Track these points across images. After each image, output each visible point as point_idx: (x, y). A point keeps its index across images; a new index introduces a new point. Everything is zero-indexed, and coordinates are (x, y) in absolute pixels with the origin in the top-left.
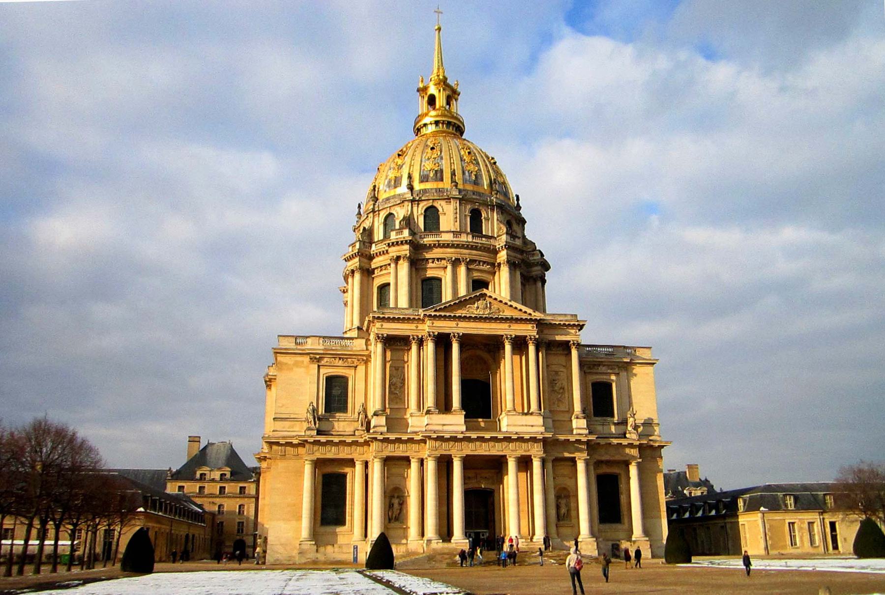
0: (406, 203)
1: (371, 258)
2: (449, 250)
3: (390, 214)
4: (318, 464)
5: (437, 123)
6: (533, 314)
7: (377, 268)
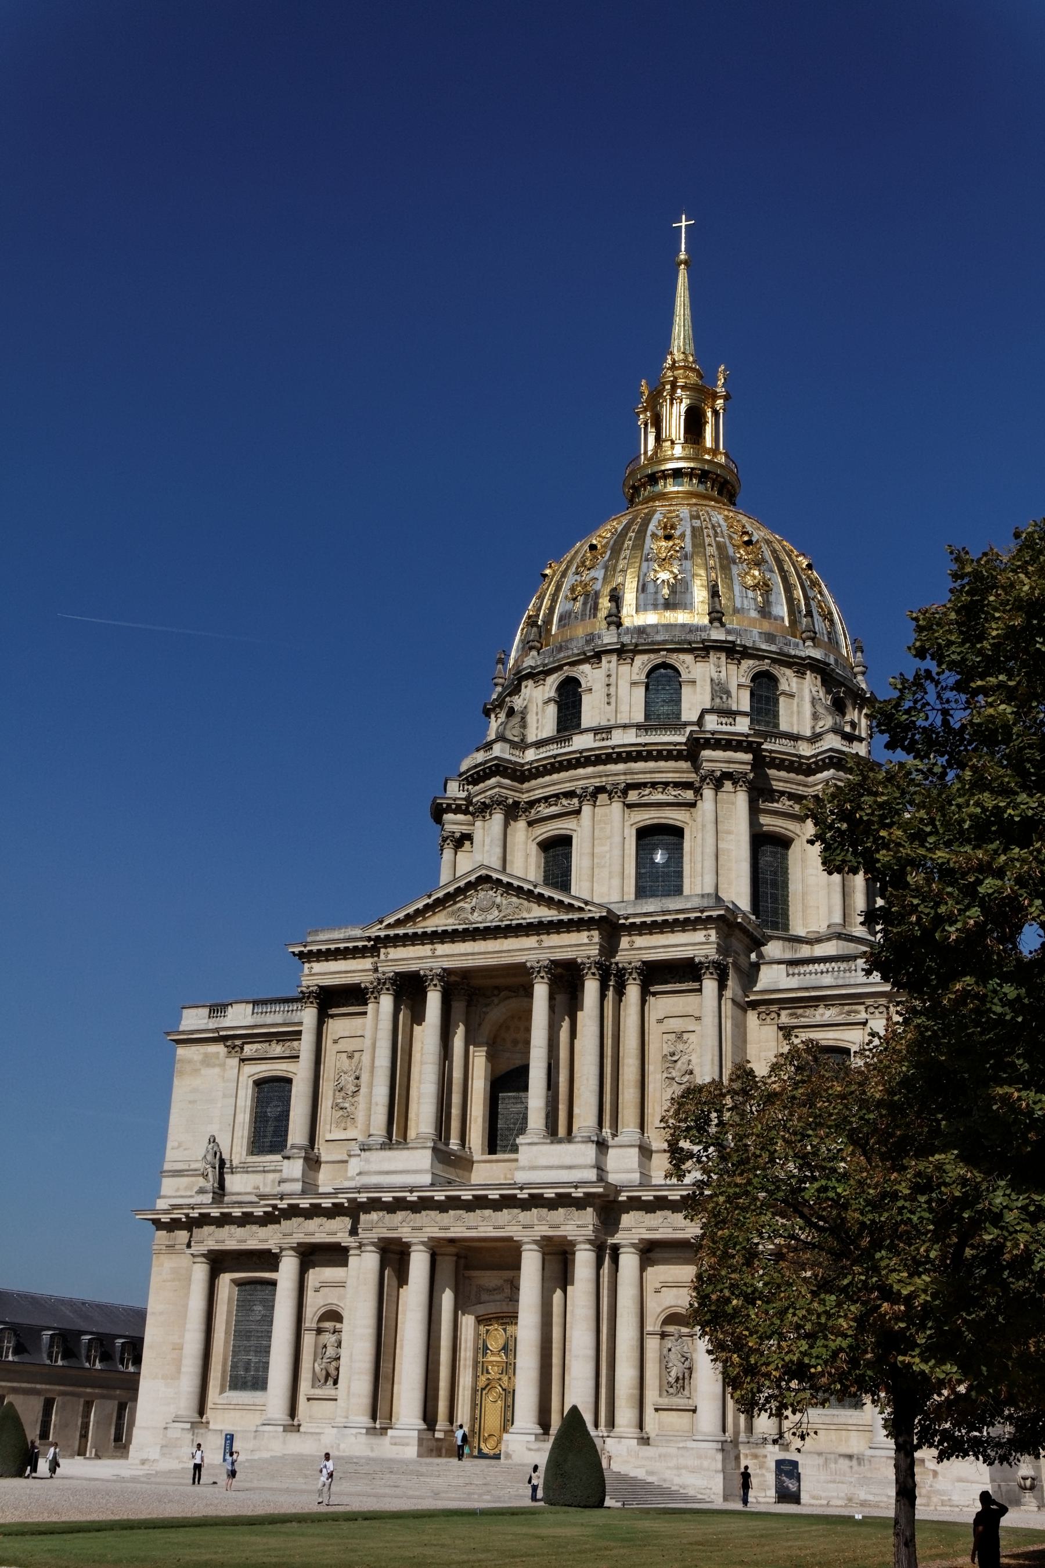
2: (581, 771)
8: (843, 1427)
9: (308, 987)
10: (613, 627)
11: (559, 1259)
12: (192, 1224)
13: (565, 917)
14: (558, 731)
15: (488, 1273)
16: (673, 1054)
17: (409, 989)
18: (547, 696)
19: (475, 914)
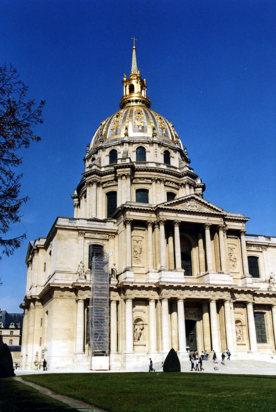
0: (125, 144)
2: (153, 173)
5: (136, 101)
7: (105, 182)
8: (266, 348)
13: (217, 213)
14: (137, 160)
16: (230, 253)
18: (133, 150)
19: (190, 208)
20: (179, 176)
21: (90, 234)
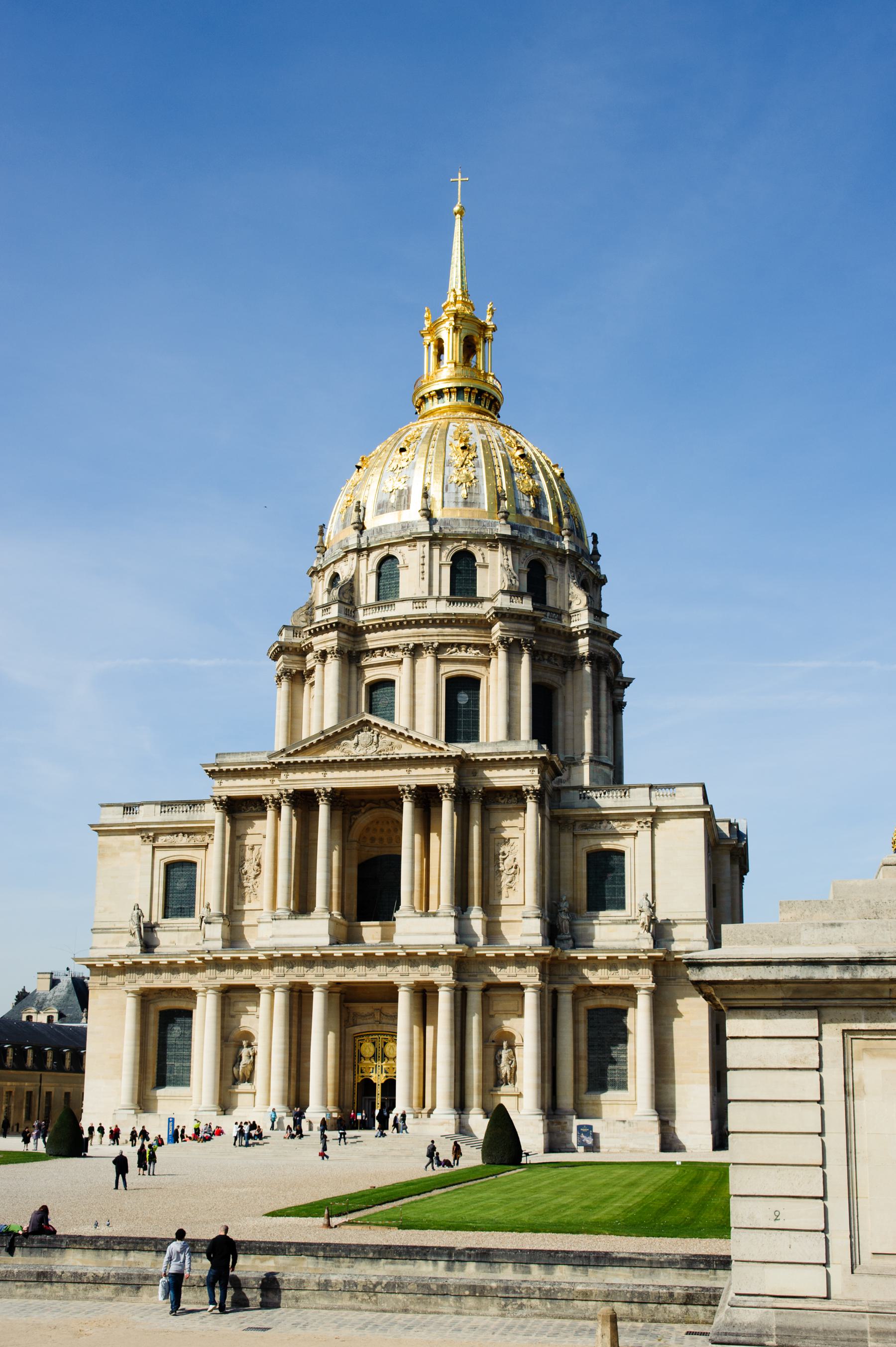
0: (350, 556)
1: (302, 652)
3: (336, 576)
4: (145, 998)
5: (440, 394)
6: (445, 748)
9: (220, 797)
10: (424, 519)
11: (424, 995)
12: (124, 969)
13: (429, 755)
15: (363, 1005)
17: (304, 802)
18: (370, 569)
20: (482, 624)
21: (168, 837)
